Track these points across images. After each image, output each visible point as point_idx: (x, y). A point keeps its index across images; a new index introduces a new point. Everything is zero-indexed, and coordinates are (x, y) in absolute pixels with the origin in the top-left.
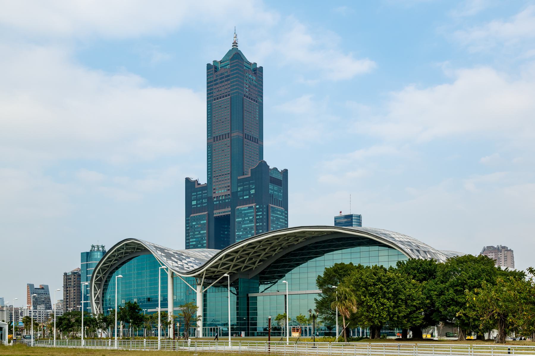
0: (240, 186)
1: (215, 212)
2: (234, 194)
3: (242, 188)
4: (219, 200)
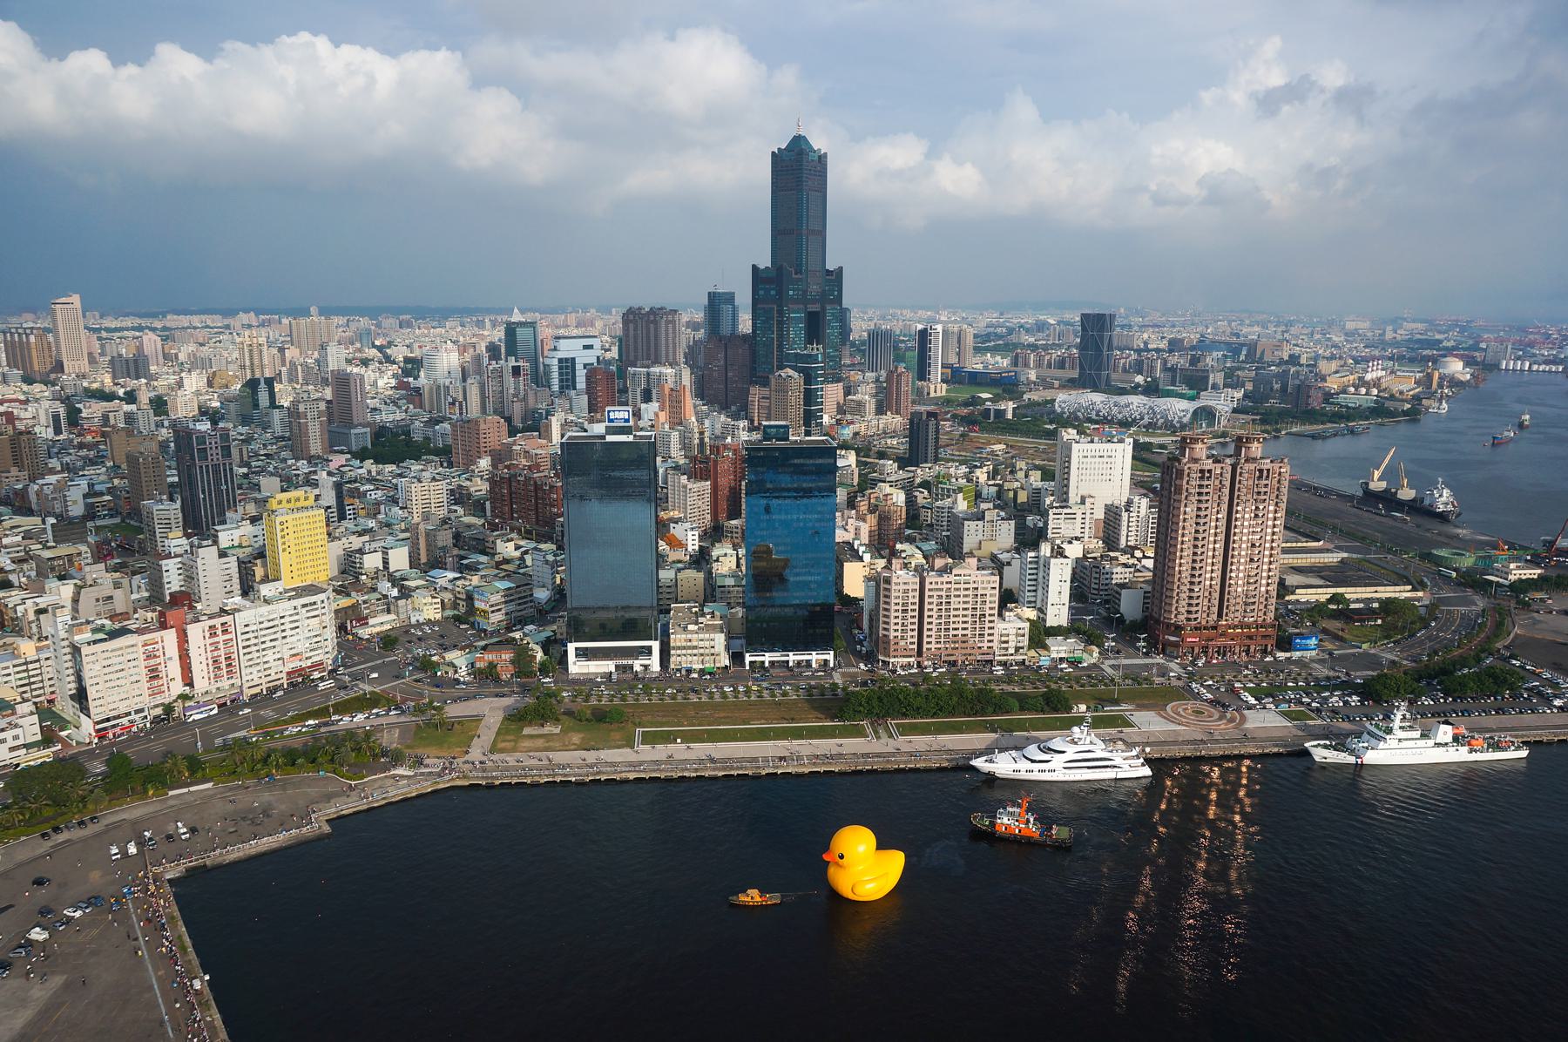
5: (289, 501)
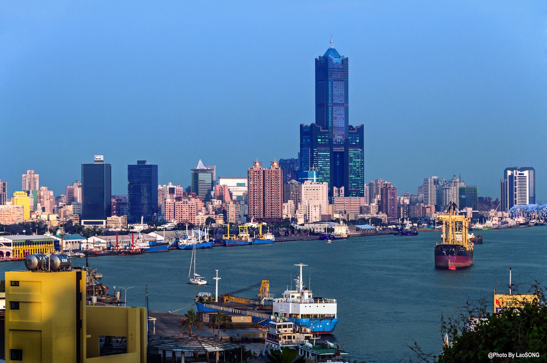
0: (350, 136)
1: (334, 148)
2: (347, 140)
3: (351, 137)
4: (337, 142)
5: (19, 194)
